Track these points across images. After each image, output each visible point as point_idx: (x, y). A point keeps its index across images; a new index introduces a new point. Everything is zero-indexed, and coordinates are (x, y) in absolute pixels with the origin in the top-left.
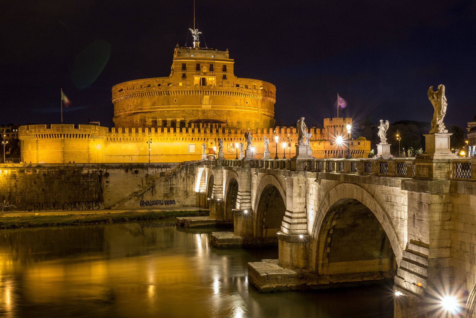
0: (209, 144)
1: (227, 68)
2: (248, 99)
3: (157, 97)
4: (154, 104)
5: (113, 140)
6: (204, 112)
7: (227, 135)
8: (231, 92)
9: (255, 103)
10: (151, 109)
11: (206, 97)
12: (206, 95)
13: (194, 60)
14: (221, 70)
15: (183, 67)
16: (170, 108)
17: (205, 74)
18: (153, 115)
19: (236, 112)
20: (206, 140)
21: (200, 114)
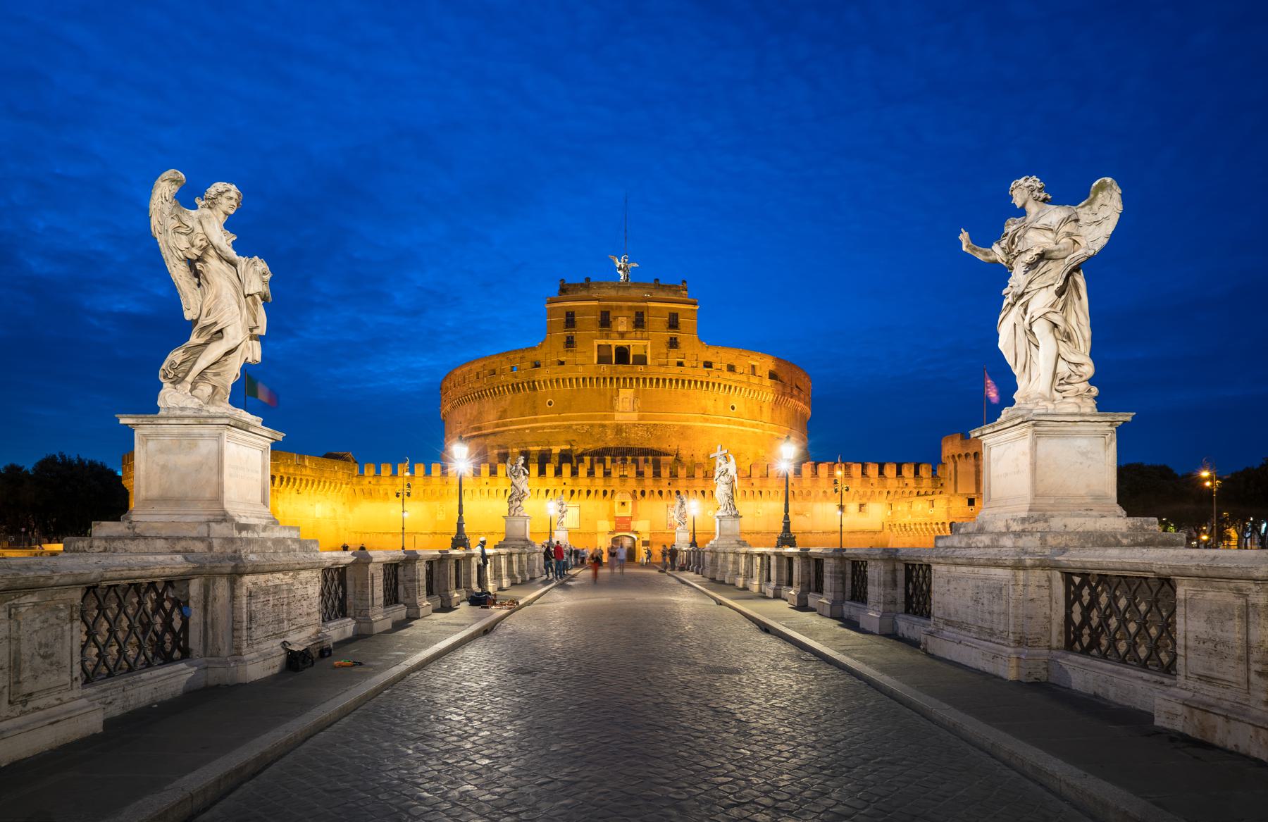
0: (617, 506)
1: (680, 320)
2: (737, 399)
3: (509, 397)
4: (503, 414)
5: (369, 495)
6: (619, 429)
7: (665, 482)
8: (690, 382)
9: (756, 409)
10: (497, 426)
11: (626, 394)
12: (625, 387)
13: (595, 303)
14: (664, 327)
15: (567, 321)
16: (536, 421)
17: (622, 335)
18: (500, 440)
19: (703, 431)
20: (609, 494)
21: (610, 434)
